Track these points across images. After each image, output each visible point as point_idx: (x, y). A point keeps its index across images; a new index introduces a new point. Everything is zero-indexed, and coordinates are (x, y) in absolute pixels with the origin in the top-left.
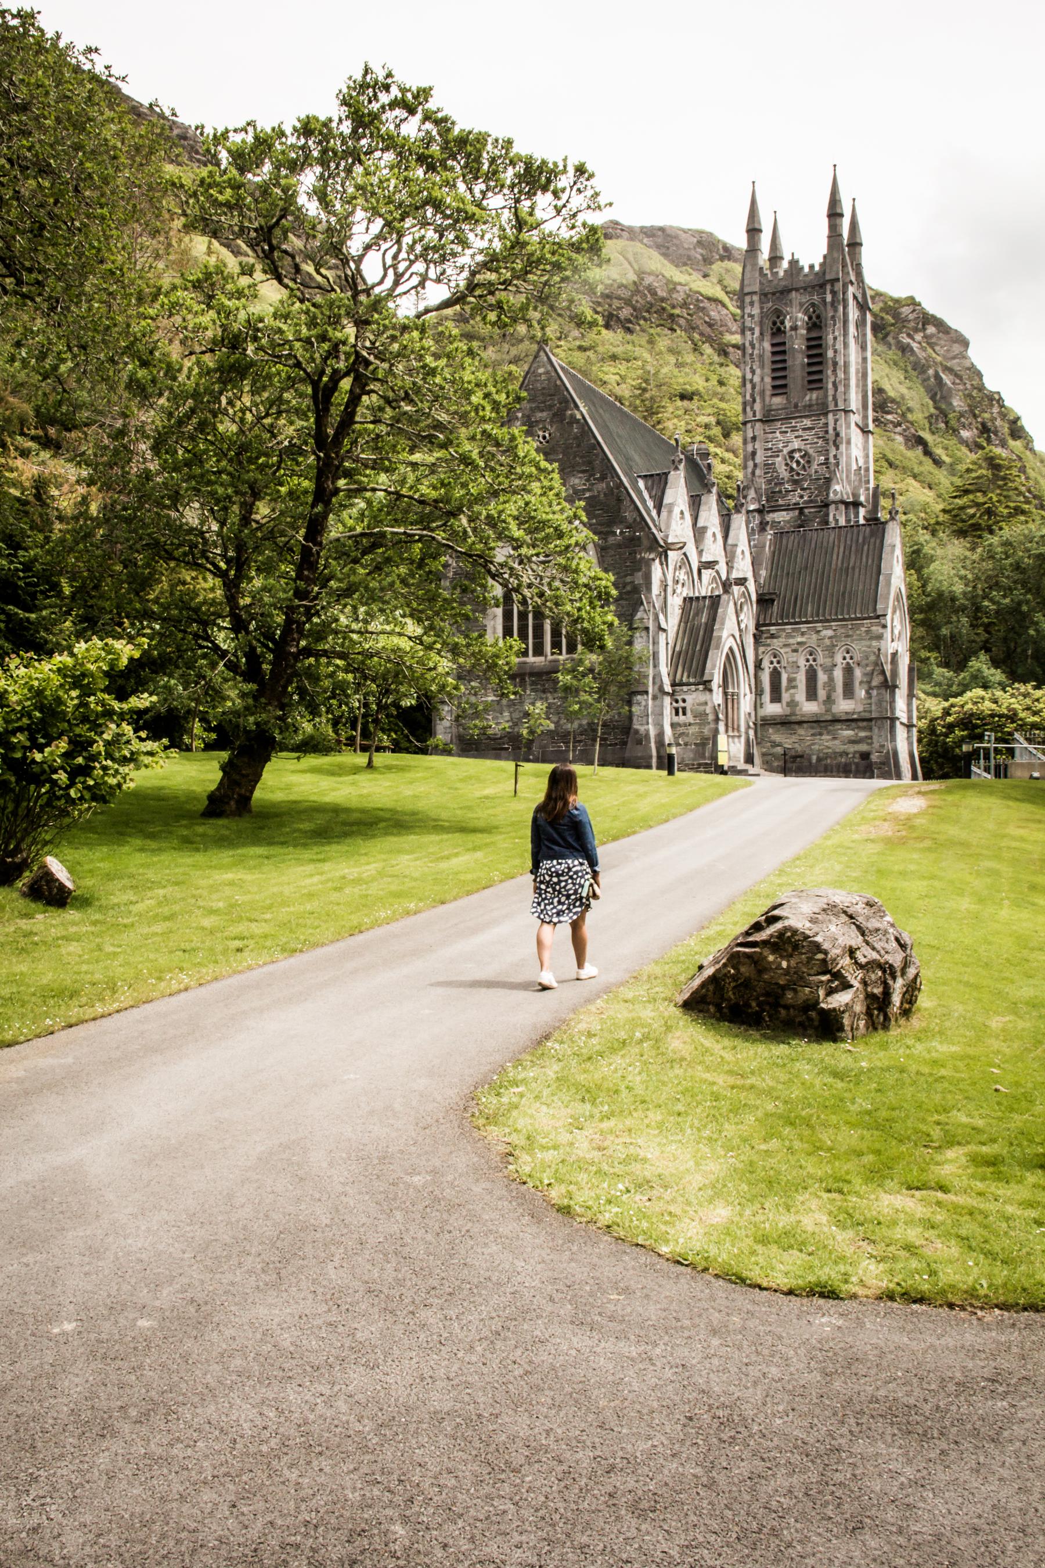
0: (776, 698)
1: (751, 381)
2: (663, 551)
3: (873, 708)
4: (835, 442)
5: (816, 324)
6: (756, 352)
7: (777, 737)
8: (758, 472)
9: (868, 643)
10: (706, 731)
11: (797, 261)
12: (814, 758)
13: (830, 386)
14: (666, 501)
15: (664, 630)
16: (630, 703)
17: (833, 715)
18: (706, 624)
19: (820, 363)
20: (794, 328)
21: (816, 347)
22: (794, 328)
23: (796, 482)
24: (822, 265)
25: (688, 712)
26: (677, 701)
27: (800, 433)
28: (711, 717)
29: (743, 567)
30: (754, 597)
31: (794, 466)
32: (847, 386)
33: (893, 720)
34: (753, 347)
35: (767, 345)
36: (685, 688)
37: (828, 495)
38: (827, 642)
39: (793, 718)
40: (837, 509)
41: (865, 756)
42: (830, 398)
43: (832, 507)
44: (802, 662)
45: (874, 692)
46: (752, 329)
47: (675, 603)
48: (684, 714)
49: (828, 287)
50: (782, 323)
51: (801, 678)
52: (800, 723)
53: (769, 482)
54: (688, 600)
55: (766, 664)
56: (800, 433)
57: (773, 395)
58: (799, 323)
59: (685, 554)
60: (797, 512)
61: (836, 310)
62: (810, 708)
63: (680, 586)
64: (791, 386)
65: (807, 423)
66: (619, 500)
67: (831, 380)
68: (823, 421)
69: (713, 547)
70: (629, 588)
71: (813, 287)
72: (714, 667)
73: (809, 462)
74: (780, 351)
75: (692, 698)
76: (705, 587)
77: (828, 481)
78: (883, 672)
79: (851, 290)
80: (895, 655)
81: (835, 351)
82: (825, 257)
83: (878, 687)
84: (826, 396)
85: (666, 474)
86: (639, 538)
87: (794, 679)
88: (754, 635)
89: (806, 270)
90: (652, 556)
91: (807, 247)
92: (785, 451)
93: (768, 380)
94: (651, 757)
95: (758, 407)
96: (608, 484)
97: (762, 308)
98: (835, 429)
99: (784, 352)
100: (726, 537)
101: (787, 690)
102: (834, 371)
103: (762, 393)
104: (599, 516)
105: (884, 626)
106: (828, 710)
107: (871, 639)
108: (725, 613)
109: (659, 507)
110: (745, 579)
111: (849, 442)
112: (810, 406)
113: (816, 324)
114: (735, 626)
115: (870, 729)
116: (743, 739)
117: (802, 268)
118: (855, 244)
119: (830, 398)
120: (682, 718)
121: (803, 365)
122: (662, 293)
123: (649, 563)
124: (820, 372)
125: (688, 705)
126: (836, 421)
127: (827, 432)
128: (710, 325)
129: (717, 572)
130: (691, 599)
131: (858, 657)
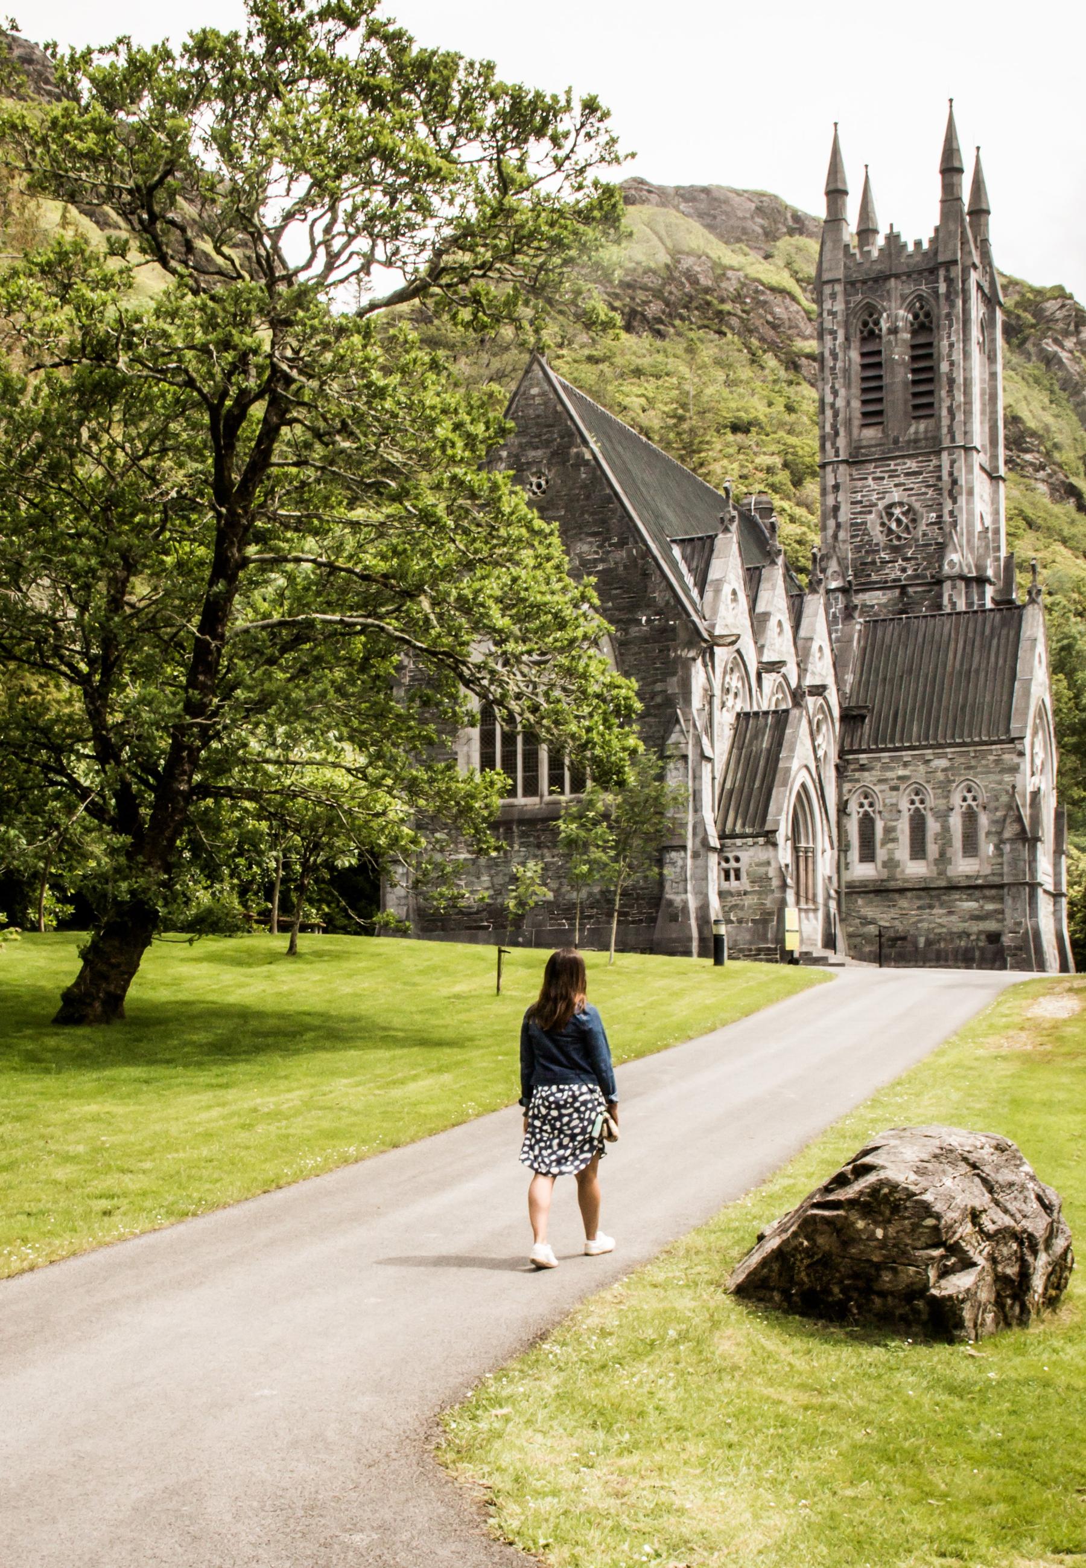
1: (833, 406)
2: (707, 646)
3: (1006, 869)
5: (924, 326)
6: (839, 364)
7: (869, 912)
8: (842, 535)
9: (998, 777)
10: (769, 903)
11: (898, 236)
12: (922, 941)
13: (944, 412)
14: (713, 575)
15: (709, 760)
16: (660, 863)
17: (949, 879)
18: (769, 751)
19: (930, 381)
20: (894, 331)
21: (924, 359)
22: (894, 331)
23: (895, 549)
24: (932, 241)
25: (744, 875)
26: (727, 860)
27: (902, 479)
28: (775, 883)
29: (822, 670)
30: (836, 713)
31: (894, 526)
32: (968, 413)
33: (1034, 886)
34: (835, 357)
35: (855, 355)
36: (739, 842)
37: (941, 567)
38: (940, 776)
39: (892, 885)
40: (954, 587)
41: (994, 938)
42: (945, 430)
43: (947, 585)
44: (904, 805)
45: (1007, 848)
46: (833, 333)
47: (725, 720)
48: (738, 878)
49: (942, 273)
50: (877, 323)
51: (903, 827)
52: (902, 891)
53: (858, 549)
54: (743, 717)
55: (853, 807)
56: (902, 479)
57: (864, 426)
58: (900, 324)
59: (738, 651)
60: (897, 592)
61: (952, 305)
62: (915, 870)
63: (731, 696)
64: (889, 412)
65: (912, 465)
66: (646, 575)
67: (946, 404)
68: (935, 462)
69: (778, 641)
70: (659, 699)
71: (920, 273)
72: (779, 812)
73: (914, 521)
74: (873, 364)
75: (749, 856)
76: (768, 698)
77: (942, 548)
78: (1019, 819)
79: (974, 276)
80: (1036, 794)
81: (952, 364)
82: (937, 230)
83: (1012, 840)
84: (938, 427)
85: (712, 538)
86: (673, 629)
87: (893, 829)
88: (837, 767)
89: (911, 248)
90: (692, 654)
91: (911, 215)
92: (881, 505)
93: (856, 404)
94: (690, 939)
95: (841, 442)
96: (629, 552)
97: (847, 302)
98: (951, 474)
99: (879, 365)
100: (796, 627)
101: (883, 844)
102: (950, 391)
103: (848, 422)
104: (617, 597)
105: (1021, 754)
106: (942, 873)
107: (1003, 771)
108: (795, 736)
109: (702, 584)
110: (824, 687)
111: (970, 493)
112: (916, 441)
113: (924, 326)
114: (809, 753)
115: (1001, 900)
116: (820, 914)
117: (905, 246)
118: (979, 212)
119: (945, 430)
120: (734, 884)
121: (905, 383)
122: (705, 281)
123: (687, 664)
124: (930, 393)
125: (743, 866)
126: (953, 463)
127: (939, 478)
128: (774, 327)
129: (785, 677)
130: (747, 714)
131: (983, 797)
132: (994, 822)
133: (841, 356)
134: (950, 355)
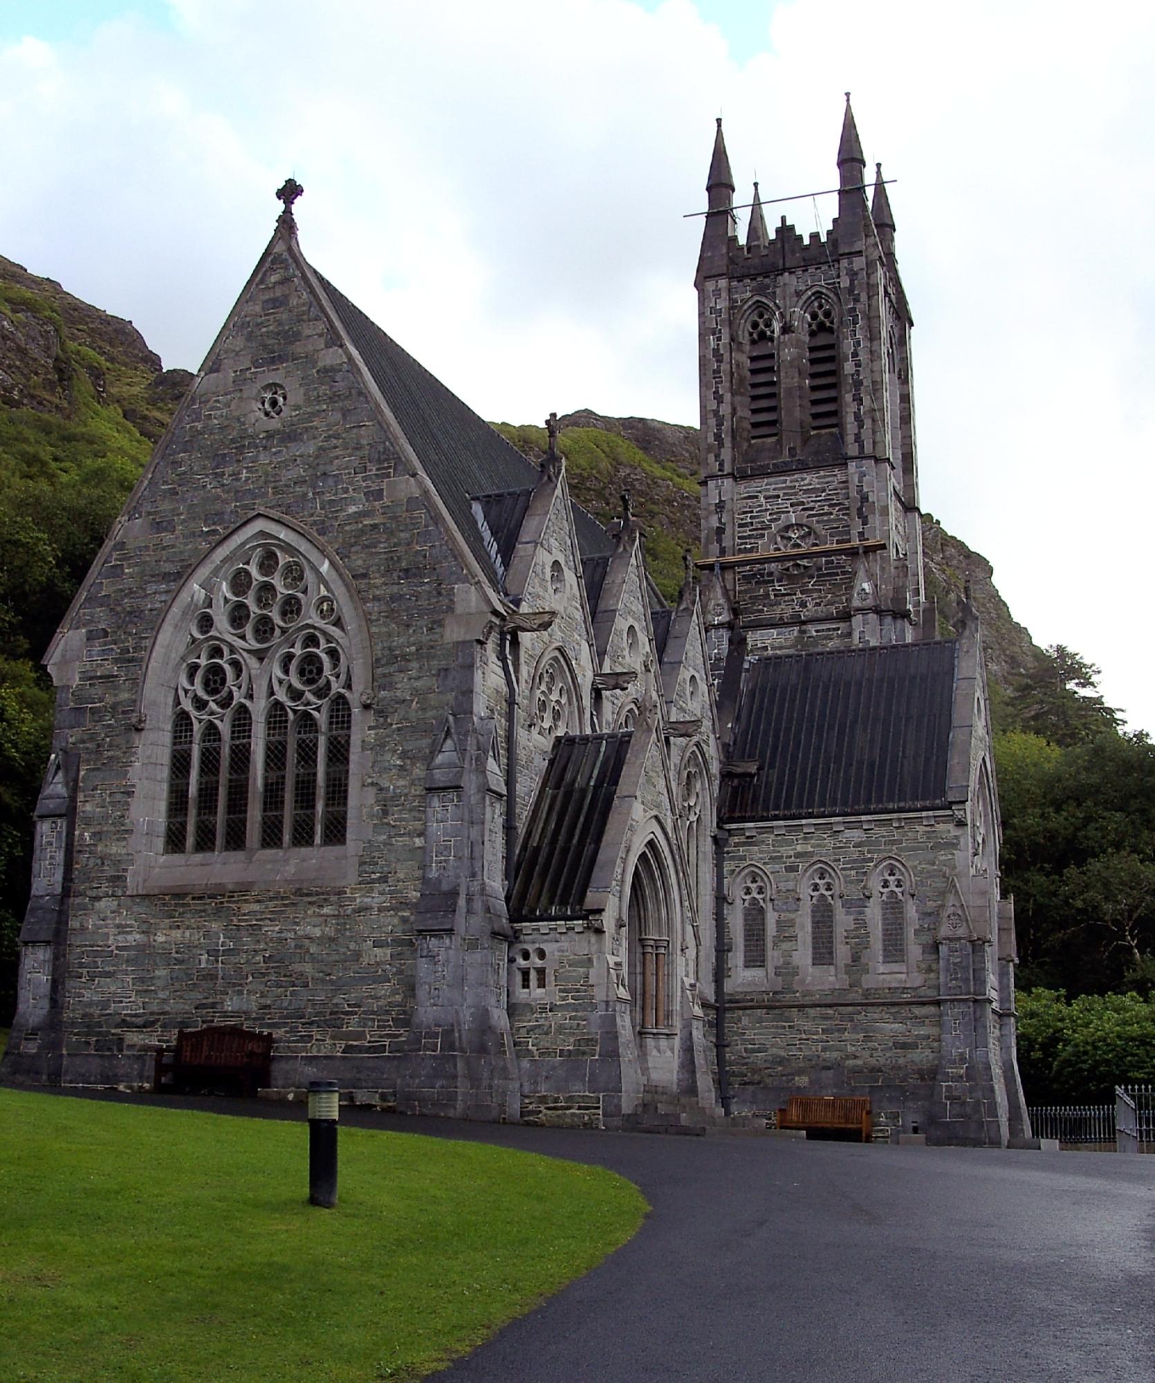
0: (755, 958)
1: (716, 413)
4: (860, 510)
9: (930, 856)
11: (792, 228)
25: (550, 978)
26: (526, 956)
30: (715, 768)
33: (981, 1002)
37: (849, 600)
40: (865, 623)
43: (857, 620)
44: (805, 891)
47: (535, 745)
48: (542, 984)
50: (768, 324)
54: (564, 745)
56: (802, 498)
61: (856, 300)
62: (821, 980)
63: (548, 716)
68: (841, 478)
81: (858, 365)
87: (791, 923)
89: (806, 241)
93: (744, 412)
95: (726, 454)
98: (860, 491)
101: (775, 944)
105: (961, 824)
107: (937, 847)
116: (677, 1042)
125: (549, 965)
126: (862, 475)
131: (910, 880)
132: (925, 915)
133: (726, 357)
134: (855, 354)
